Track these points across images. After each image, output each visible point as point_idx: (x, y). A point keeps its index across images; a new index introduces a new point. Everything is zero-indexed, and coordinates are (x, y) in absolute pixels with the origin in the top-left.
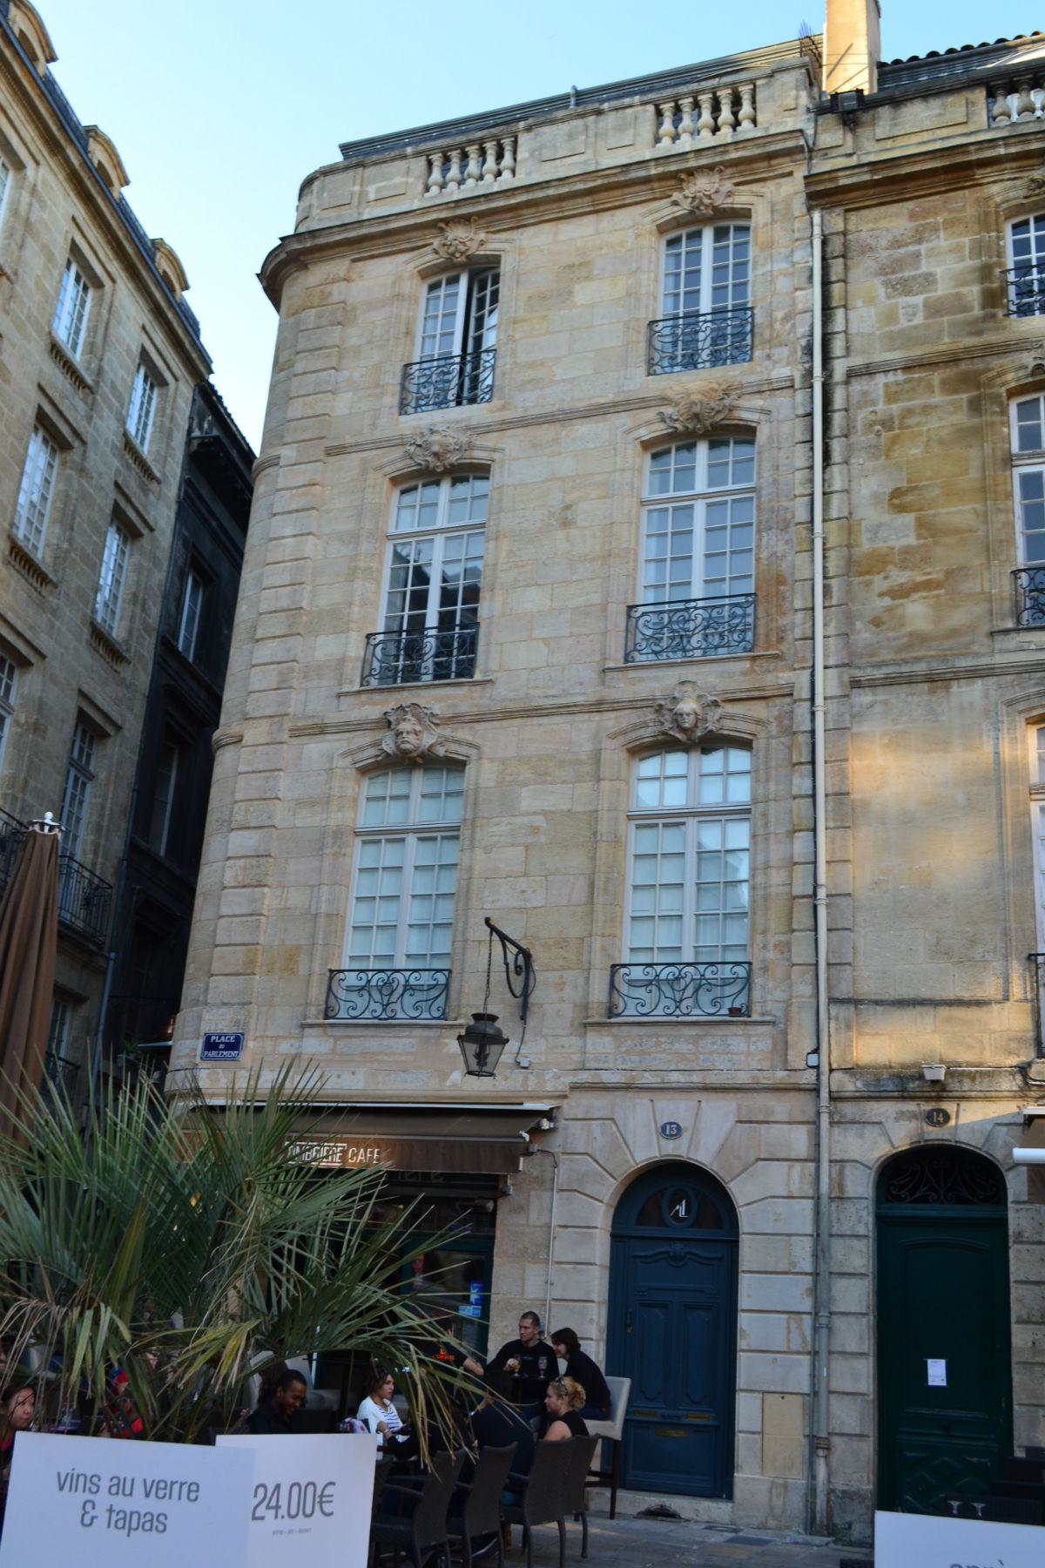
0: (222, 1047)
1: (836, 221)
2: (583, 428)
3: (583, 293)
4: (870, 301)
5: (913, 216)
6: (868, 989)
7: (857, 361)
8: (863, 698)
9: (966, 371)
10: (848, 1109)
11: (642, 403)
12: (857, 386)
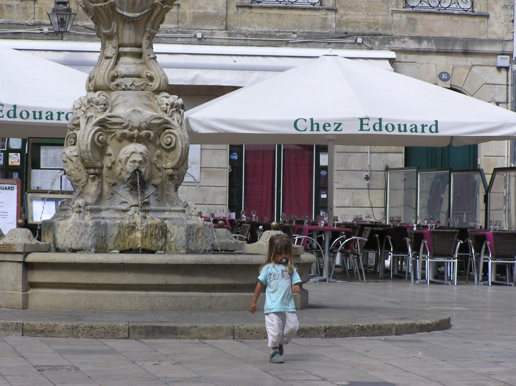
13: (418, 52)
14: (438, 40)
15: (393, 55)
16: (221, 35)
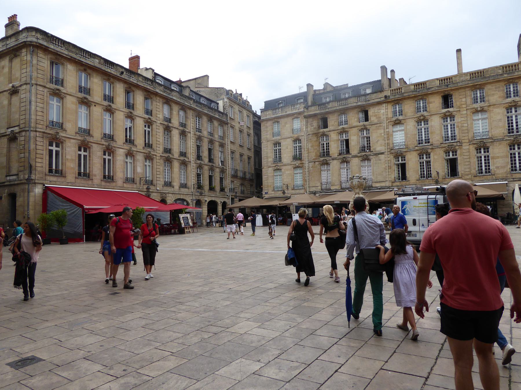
0: (266, 193)
3: (287, 126)
9: (316, 134)
11: (292, 137)
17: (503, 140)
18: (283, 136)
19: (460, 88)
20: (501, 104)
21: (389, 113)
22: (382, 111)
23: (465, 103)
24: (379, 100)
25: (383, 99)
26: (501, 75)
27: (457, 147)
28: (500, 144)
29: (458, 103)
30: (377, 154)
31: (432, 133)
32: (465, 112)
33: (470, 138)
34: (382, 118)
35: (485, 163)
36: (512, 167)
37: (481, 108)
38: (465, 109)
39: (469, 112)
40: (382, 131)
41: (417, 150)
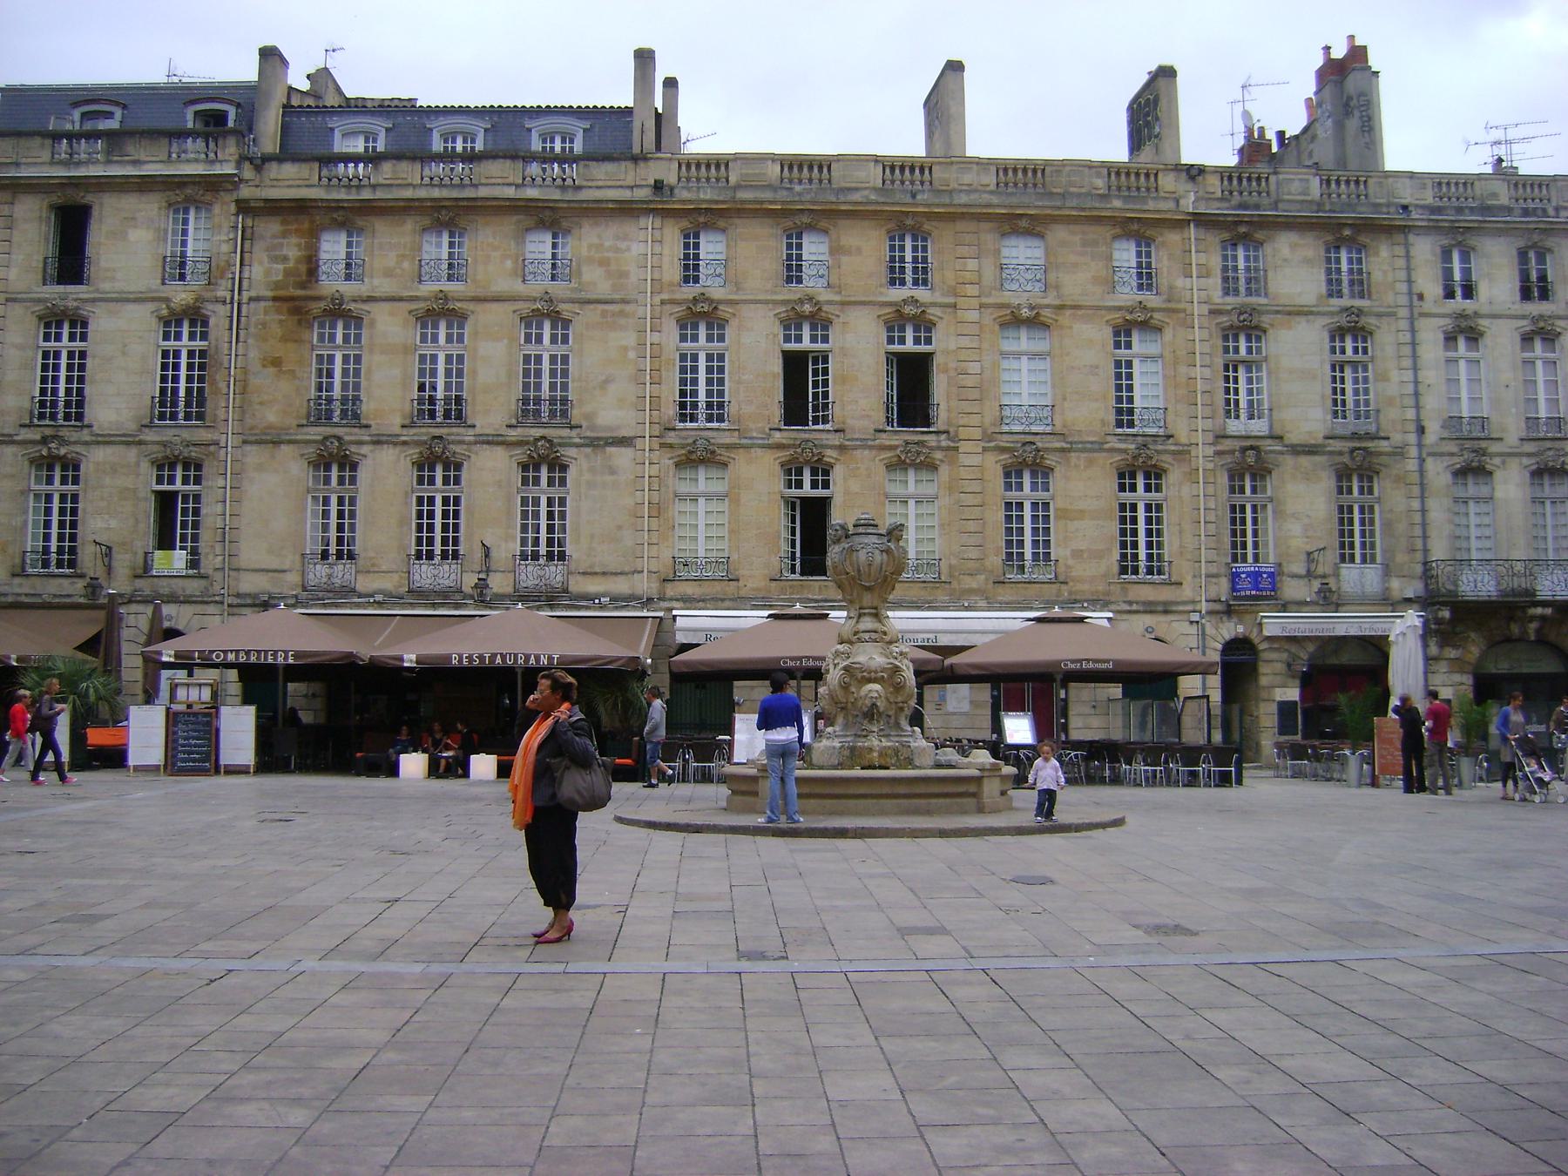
1: (249, 222)
2: (130, 307)
4: (261, 263)
5: (284, 223)
6: (243, 565)
7: (253, 294)
8: (248, 448)
10: (236, 610)
12: (253, 305)
13: (1129, 612)
14: (1144, 603)
15: (1110, 615)
16: (983, 604)
17: (1099, 447)
18: (106, 286)
19: (963, 216)
20: (1099, 308)
21: (666, 260)
22: (637, 249)
23: (974, 278)
24: (626, 195)
25: (643, 194)
26: (1102, 196)
27: (938, 455)
28: (1090, 463)
29: (950, 276)
30: (598, 443)
31: (843, 380)
32: (973, 316)
33: (988, 420)
34: (633, 278)
35: (1035, 531)
36: (1124, 556)
37: (1032, 308)
38: (975, 302)
39: (988, 318)
40: (630, 339)
41: (780, 447)
